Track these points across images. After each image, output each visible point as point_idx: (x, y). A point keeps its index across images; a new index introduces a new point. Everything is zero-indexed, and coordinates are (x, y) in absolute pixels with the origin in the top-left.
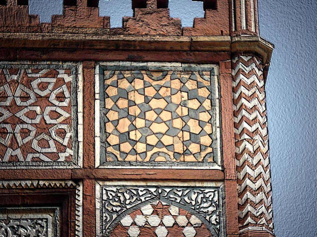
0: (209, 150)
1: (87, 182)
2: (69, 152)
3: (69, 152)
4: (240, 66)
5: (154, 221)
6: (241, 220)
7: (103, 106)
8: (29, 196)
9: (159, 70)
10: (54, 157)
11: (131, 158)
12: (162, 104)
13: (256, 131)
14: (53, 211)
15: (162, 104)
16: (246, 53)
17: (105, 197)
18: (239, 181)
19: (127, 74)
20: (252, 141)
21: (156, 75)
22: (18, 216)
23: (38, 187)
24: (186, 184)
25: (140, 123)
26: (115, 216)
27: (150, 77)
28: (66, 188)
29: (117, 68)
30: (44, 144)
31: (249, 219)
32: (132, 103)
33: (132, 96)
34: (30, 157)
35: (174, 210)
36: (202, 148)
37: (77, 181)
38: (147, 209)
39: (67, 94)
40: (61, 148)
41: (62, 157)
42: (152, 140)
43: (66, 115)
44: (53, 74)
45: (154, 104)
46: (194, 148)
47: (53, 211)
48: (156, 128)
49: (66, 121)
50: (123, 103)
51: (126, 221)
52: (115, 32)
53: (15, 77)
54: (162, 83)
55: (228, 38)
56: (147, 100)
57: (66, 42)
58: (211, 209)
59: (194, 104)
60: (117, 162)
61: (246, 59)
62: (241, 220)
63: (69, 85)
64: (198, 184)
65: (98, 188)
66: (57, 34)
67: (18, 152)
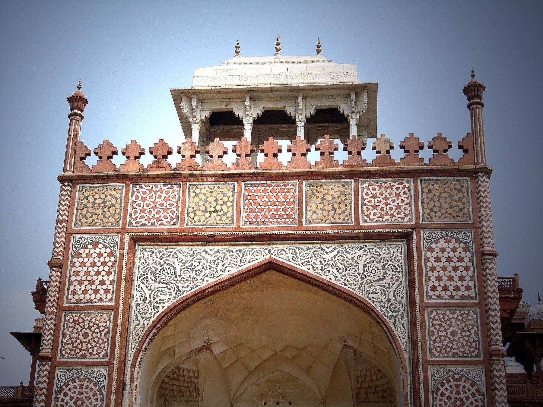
0: (467, 215)
1: (417, 229)
2: (409, 217)
3: (409, 217)
4: (479, 178)
5: (445, 245)
6: (481, 244)
7: (422, 196)
8: (394, 236)
9: (444, 181)
10: (403, 219)
11: (434, 219)
12: (446, 195)
13: (487, 207)
14: (404, 241)
15: (446, 195)
16: (482, 172)
17: (425, 236)
18: (480, 228)
19: (432, 183)
20: (485, 211)
21: (444, 183)
22: (389, 243)
23: (398, 232)
24: (458, 230)
25: (438, 204)
26: (429, 244)
27: (442, 183)
28: (409, 232)
29: (427, 180)
30: (399, 213)
31: (485, 245)
32: (434, 195)
33: (434, 192)
34: (394, 219)
35: (453, 241)
36: (465, 214)
37: (413, 229)
38: (442, 241)
39: (407, 192)
40: (406, 215)
41: (407, 219)
42: (443, 211)
43: (407, 201)
44: (401, 183)
45: (443, 195)
46: (460, 214)
47: (404, 241)
48: (444, 206)
49: (408, 204)
50: (430, 195)
51: (434, 246)
52: (426, 165)
53: (386, 185)
54: (447, 186)
55: (473, 166)
56: (440, 194)
57: (406, 170)
58: (468, 240)
59: (460, 195)
60: (429, 221)
61: (482, 174)
62: (481, 244)
63: (408, 188)
64: (463, 230)
65: (421, 232)
66: (402, 167)
67: (389, 217)
